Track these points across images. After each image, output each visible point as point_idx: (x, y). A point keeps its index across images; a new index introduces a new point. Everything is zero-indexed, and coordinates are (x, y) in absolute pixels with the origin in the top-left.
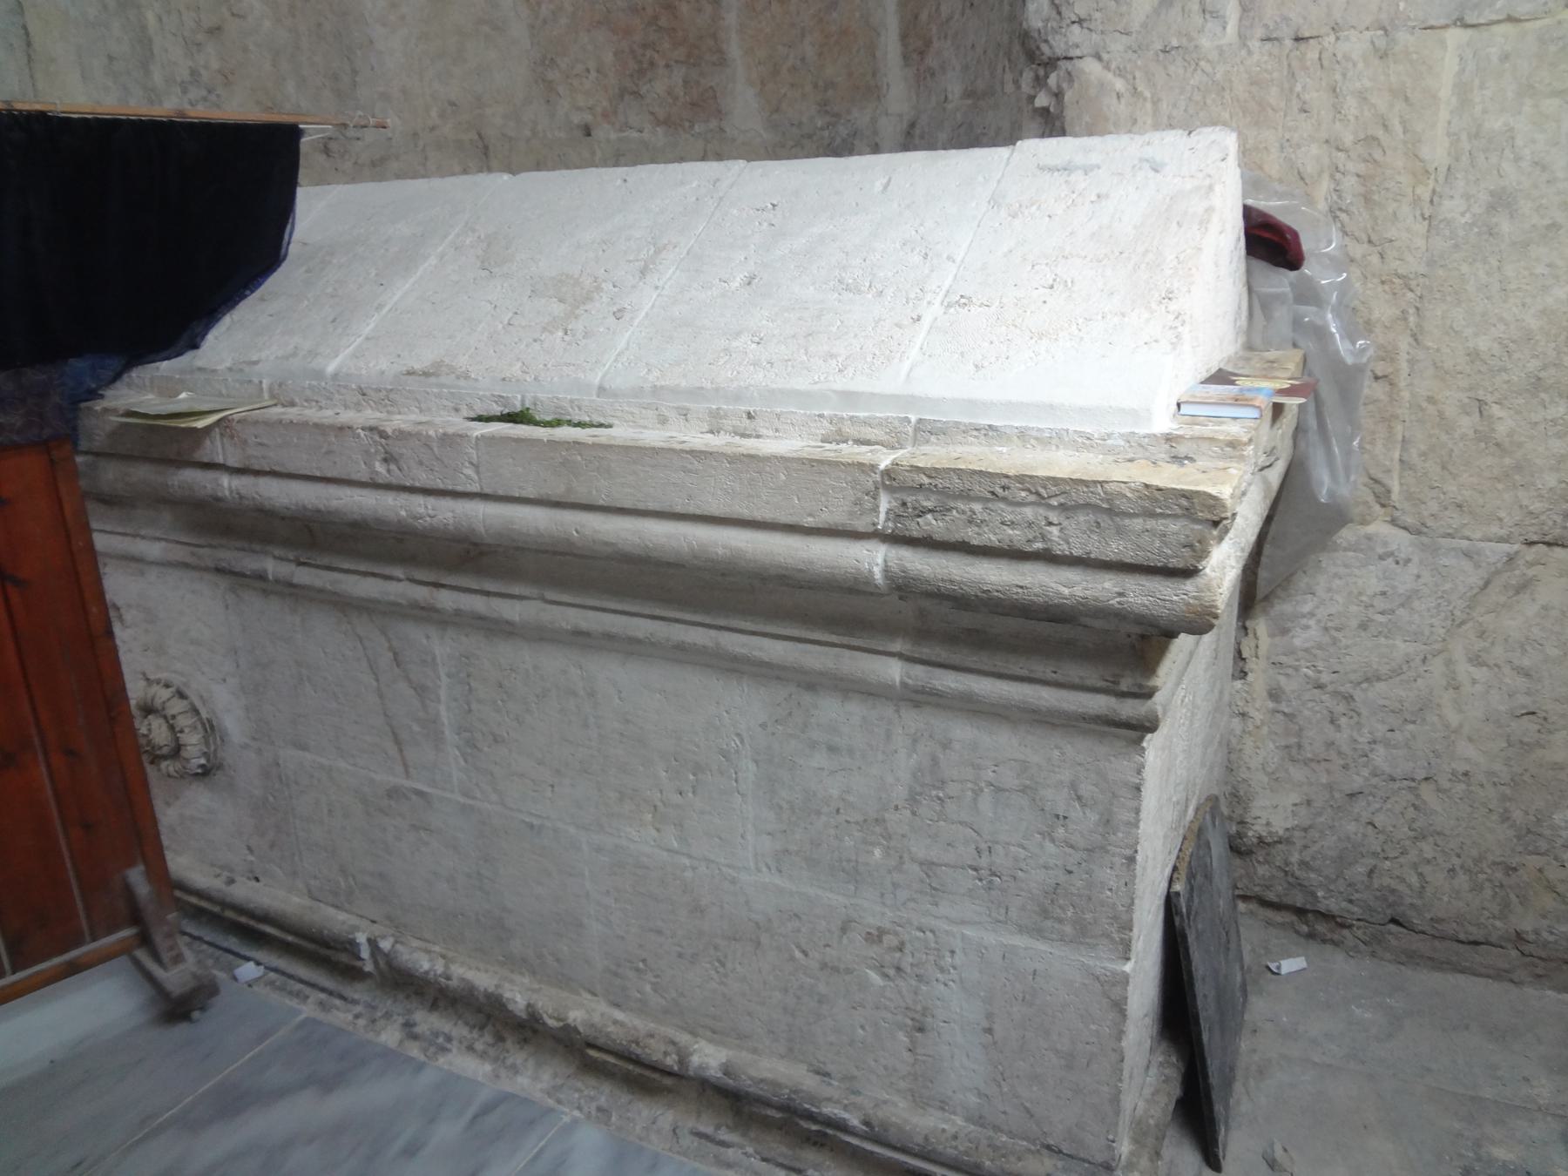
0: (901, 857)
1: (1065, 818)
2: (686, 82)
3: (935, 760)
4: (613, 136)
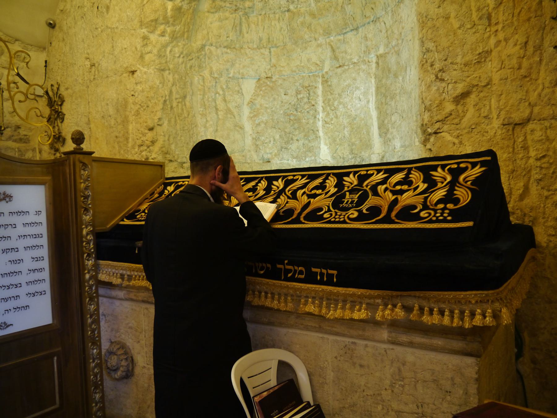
0: (388, 409)
1: (450, 392)
2: (303, 144)
3: (400, 370)
4: (278, 162)
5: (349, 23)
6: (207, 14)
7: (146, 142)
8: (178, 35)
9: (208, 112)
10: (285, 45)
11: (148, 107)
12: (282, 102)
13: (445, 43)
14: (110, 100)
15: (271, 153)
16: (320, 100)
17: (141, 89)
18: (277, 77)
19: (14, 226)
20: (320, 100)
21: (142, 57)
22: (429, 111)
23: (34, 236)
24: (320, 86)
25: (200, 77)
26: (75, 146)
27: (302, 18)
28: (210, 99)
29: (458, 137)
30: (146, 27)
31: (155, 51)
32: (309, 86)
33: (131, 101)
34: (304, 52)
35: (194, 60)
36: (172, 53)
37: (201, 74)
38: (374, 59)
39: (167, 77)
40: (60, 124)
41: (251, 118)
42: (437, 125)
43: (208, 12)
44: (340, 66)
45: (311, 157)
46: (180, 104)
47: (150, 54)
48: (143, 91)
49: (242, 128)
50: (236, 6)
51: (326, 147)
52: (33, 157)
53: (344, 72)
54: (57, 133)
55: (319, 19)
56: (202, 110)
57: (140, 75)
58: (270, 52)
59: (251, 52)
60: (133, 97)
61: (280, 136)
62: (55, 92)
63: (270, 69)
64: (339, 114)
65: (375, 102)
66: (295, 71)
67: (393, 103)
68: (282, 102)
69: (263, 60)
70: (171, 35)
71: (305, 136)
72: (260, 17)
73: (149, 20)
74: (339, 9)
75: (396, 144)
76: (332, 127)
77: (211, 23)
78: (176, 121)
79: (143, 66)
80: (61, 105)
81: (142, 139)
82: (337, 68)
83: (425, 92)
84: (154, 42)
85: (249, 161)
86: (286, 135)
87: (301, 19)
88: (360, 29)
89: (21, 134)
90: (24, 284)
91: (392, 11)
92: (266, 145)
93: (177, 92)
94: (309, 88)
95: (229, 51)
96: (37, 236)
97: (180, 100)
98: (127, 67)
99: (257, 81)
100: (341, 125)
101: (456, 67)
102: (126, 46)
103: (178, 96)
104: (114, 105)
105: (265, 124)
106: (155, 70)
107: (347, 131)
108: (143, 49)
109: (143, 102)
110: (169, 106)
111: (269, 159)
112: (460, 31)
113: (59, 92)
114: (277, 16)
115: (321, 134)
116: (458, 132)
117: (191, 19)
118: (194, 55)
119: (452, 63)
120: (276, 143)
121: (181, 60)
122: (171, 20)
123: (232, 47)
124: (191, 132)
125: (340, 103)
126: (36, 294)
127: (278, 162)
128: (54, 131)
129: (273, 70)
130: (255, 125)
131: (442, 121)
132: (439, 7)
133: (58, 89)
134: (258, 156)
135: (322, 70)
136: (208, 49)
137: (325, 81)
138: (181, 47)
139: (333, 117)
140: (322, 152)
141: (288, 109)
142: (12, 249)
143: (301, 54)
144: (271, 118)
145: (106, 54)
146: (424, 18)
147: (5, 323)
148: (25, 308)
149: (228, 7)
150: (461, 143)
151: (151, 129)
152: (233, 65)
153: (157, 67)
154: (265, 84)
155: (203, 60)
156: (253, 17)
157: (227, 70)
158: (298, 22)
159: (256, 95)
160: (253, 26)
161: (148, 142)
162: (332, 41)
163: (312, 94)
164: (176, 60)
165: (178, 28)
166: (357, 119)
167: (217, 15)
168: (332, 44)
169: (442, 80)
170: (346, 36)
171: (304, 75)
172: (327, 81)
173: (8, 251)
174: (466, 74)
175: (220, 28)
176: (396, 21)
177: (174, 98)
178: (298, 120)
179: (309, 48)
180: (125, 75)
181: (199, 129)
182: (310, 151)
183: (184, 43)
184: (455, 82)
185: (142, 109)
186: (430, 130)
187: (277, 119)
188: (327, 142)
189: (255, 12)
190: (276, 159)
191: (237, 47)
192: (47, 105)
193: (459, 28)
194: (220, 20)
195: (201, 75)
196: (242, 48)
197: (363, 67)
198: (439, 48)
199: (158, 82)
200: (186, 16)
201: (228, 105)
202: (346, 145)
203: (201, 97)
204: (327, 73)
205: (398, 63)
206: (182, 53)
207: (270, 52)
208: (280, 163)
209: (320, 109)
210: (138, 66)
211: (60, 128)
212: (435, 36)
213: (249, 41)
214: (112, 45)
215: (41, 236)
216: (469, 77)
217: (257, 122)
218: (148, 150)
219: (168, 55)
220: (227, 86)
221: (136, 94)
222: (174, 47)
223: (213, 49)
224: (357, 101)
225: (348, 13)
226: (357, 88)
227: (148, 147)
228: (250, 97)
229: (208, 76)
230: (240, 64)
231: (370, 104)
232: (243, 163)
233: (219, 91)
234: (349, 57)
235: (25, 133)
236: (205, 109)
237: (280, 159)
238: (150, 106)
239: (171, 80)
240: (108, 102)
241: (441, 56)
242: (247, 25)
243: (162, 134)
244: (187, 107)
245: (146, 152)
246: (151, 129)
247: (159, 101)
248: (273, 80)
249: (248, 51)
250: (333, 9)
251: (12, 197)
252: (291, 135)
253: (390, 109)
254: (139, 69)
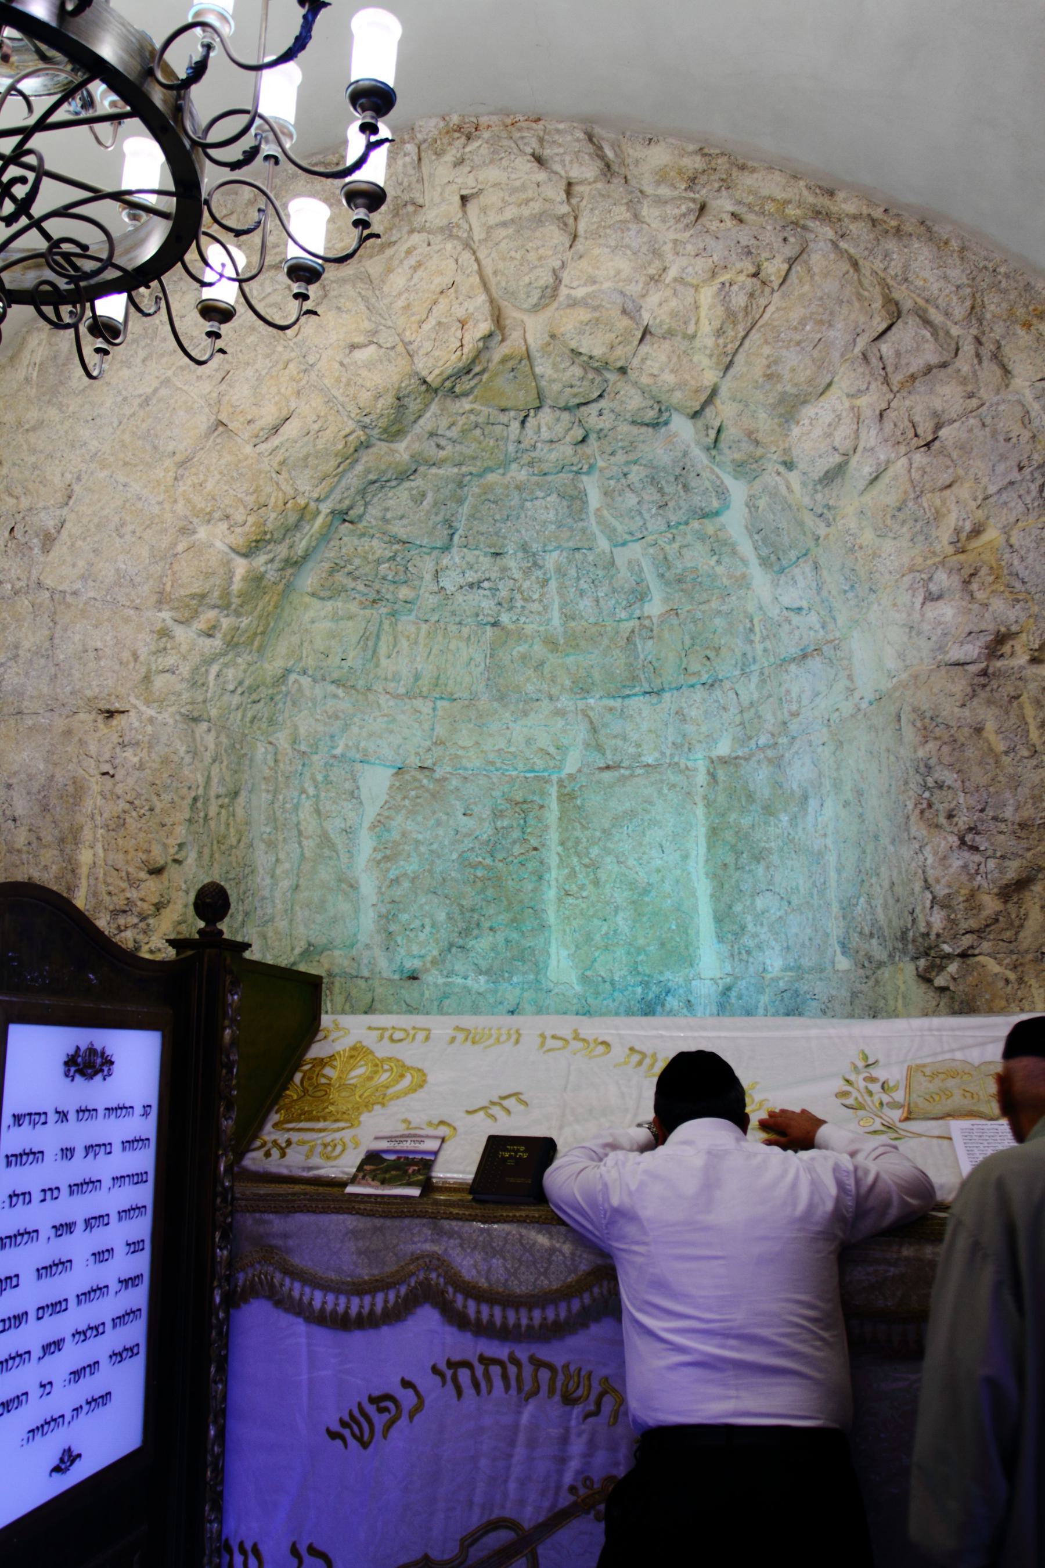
2: (507, 941)
4: (441, 981)
5: (642, 677)
6: (307, 599)
7: (139, 903)
8: (243, 639)
9: (280, 838)
10: (474, 698)
11: (151, 810)
12: (457, 832)
13: (978, 777)
14: (23, 776)
15: (422, 957)
16: (553, 837)
17: (136, 760)
18: (449, 769)
20: (553, 837)
21: (147, 679)
22: (942, 907)
24: (554, 805)
25: (270, 748)
26: (202, 924)
27: (526, 646)
28: (288, 806)
29: (1015, 967)
30: (172, 609)
31: (185, 670)
32: (525, 802)
33: (96, 788)
34: (519, 723)
35: (262, 703)
36: (221, 679)
37: (271, 739)
38: (702, 766)
39: (202, 738)
41: (379, 862)
42: (967, 941)
43: (313, 595)
44: (608, 768)
45: (525, 973)
46: (223, 811)
47: (168, 675)
48: (141, 767)
49: (354, 886)
50: (378, 592)
51: (564, 953)
53: (619, 780)
55: (567, 655)
56: (268, 830)
57: (136, 724)
58: (434, 709)
59: (392, 703)
60: (108, 781)
61: (450, 917)
63: (430, 750)
64: (603, 876)
65: (707, 861)
66: (493, 763)
67: (760, 870)
68: (457, 832)
69: (416, 725)
70: (229, 638)
71: (514, 920)
72: (424, 627)
73: (188, 592)
74: (623, 643)
75: (768, 962)
76: (584, 906)
77: (313, 622)
78: (212, 856)
79: (148, 703)
81: (129, 895)
82: (601, 769)
83: (933, 868)
84: (184, 648)
85: (366, 973)
86: (462, 913)
87: (522, 648)
88: (667, 695)
91: (762, 673)
92: (412, 935)
93: (222, 780)
94: (525, 806)
95: (340, 692)
97: (227, 800)
98: (96, 698)
99: (397, 774)
100: (608, 903)
101: (1002, 826)
102: (99, 645)
103: (222, 791)
104: (34, 790)
105: (413, 880)
106: (178, 717)
107: (626, 920)
108: (153, 658)
109: (139, 795)
110: (202, 814)
111: (414, 971)
112: (1006, 760)
114: (465, 631)
115: (552, 917)
116: (1014, 957)
117: (276, 607)
118: (264, 692)
119: (995, 818)
120: (438, 931)
121: (236, 699)
122: (236, 601)
123: (349, 684)
124: (242, 888)
125: (608, 851)
127: (441, 981)
129: (437, 751)
130: (387, 883)
131: (979, 933)
132: (963, 705)
134: (391, 960)
135: (560, 769)
136: (296, 681)
137: (566, 797)
138: (242, 667)
139: (587, 882)
140: (553, 963)
141: (472, 849)
143: (511, 725)
144: (427, 867)
145: (21, 652)
146: (927, 721)
149: (359, 592)
150: (1021, 980)
151: (157, 871)
152: (346, 727)
153: (183, 710)
154: (417, 784)
155: (280, 705)
156: (406, 624)
157: (332, 737)
158: (514, 653)
159: (390, 807)
160: (404, 644)
161: (145, 906)
162: (592, 709)
163: (531, 821)
164: (226, 697)
165: (245, 621)
166: (654, 893)
167: (329, 604)
168: (591, 714)
169: (975, 849)
170: (627, 702)
171: (514, 773)
172: (572, 796)
174: (1024, 844)
175: (332, 635)
176: (770, 696)
177: (212, 794)
178: (497, 881)
179: (532, 714)
180: (82, 716)
181: (259, 880)
182: (523, 960)
183: (249, 658)
184: (1003, 857)
185: (134, 814)
186: (947, 948)
187: (442, 873)
188: (569, 939)
189: (414, 613)
190: (434, 972)
191: (359, 687)
193: (1006, 753)
194: (336, 618)
195: (271, 743)
196: (369, 689)
197: (671, 777)
198: (967, 784)
199: (182, 749)
200: (267, 598)
201: (325, 824)
202: (620, 952)
203: (270, 797)
204: (571, 776)
205: (777, 785)
206: (241, 683)
207: (434, 709)
208: (446, 984)
209: (553, 861)
210: (133, 700)
212: (958, 760)
213: (390, 676)
214: (47, 632)
216: (1029, 849)
217: (392, 875)
218: (142, 925)
219: (211, 684)
220: (326, 777)
221: (120, 774)
222: (226, 665)
223: (305, 681)
224: (655, 853)
225: (642, 656)
226: (653, 823)
227: (143, 918)
228: (378, 810)
229: (286, 746)
230: (361, 727)
231: (691, 863)
232: (353, 977)
233: (306, 785)
234: (632, 750)
236: (276, 828)
237: (445, 972)
238: (158, 810)
239: (212, 746)
240: (14, 781)
241: (972, 802)
242: (391, 639)
243: (184, 887)
244: (239, 820)
245: (136, 931)
246: (157, 871)
247: (183, 798)
248: (437, 776)
249: (383, 699)
250: (606, 641)
252: (476, 916)
253: (750, 881)
254: (135, 707)
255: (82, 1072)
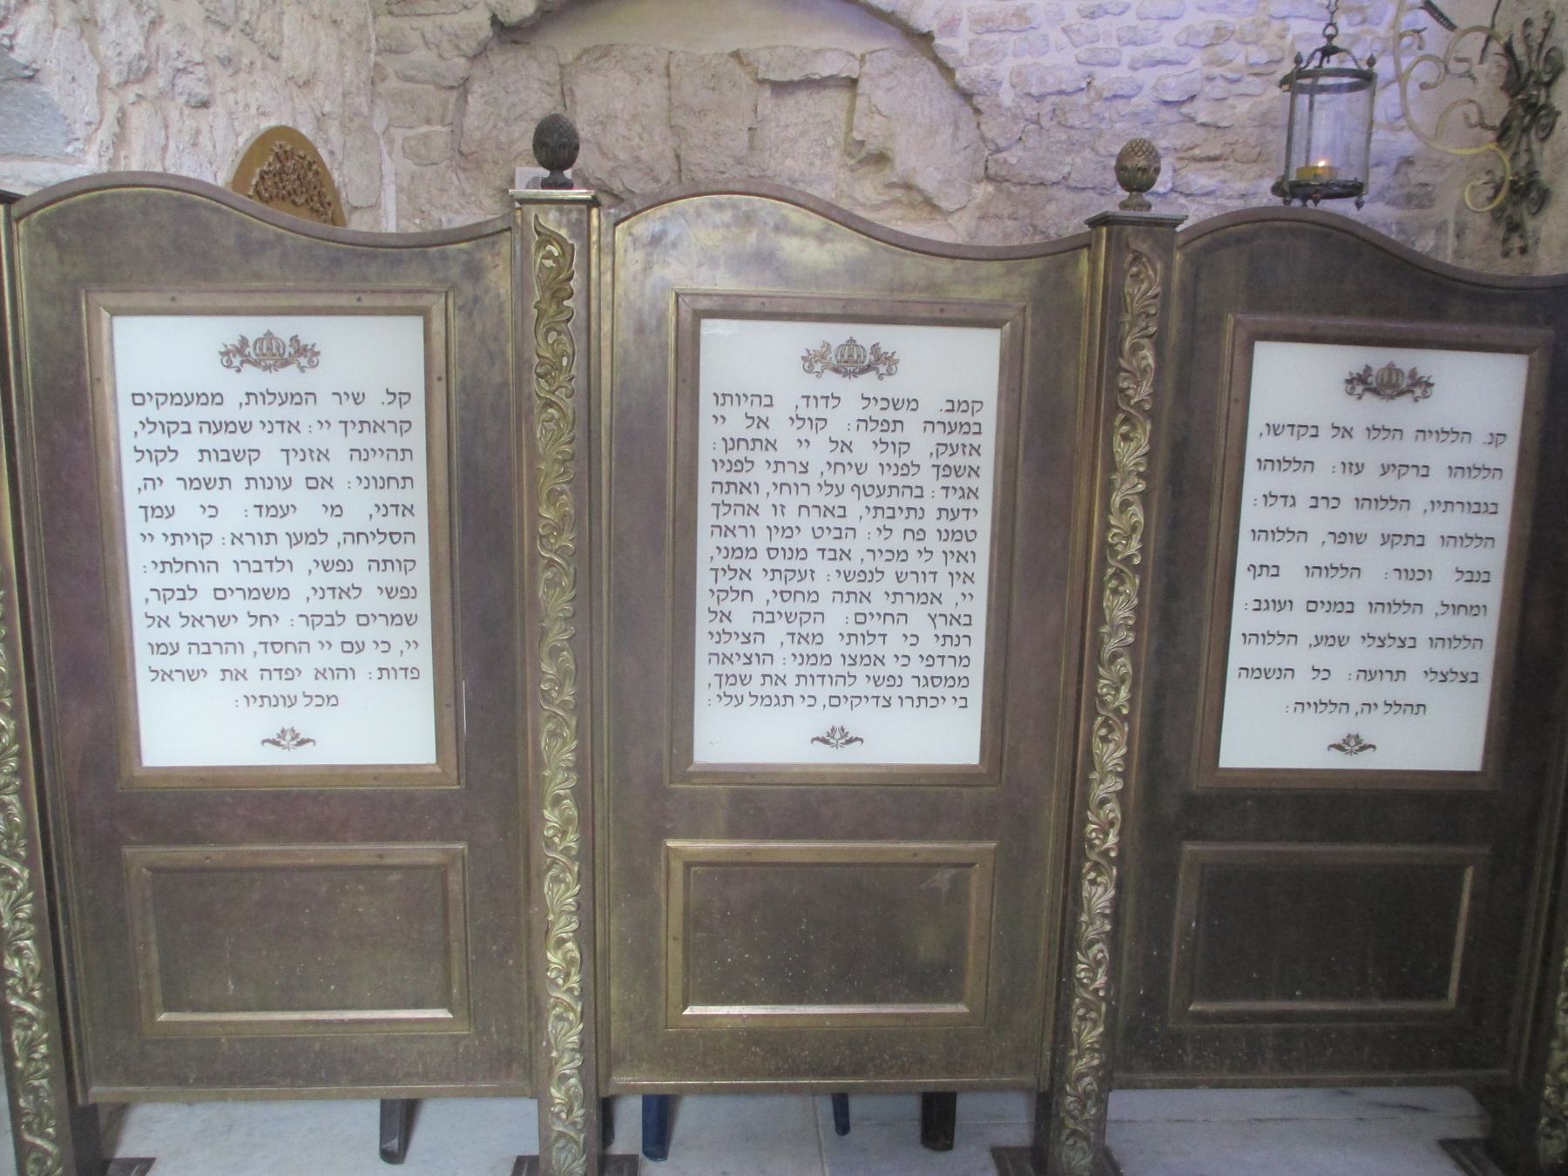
19: (1424, 471)
23: (1475, 508)
40: (1536, 146)
52: (1436, 247)
54: (1523, 174)
62: (1535, 46)
80: (1549, 84)
89: (1413, 181)
90: (1423, 643)
96: (1483, 508)
113: (1549, 44)
126: (1451, 677)
128: (1512, 167)
133: (1546, 32)
142: (1407, 536)
147: (1357, 736)
148: (1415, 710)
173: (1397, 539)
192: (1502, 88)
211: (1537, 158)
215: (1492, 509)
235: (1423, 178)
251: (1430, 385)
255: (1375, 392)
